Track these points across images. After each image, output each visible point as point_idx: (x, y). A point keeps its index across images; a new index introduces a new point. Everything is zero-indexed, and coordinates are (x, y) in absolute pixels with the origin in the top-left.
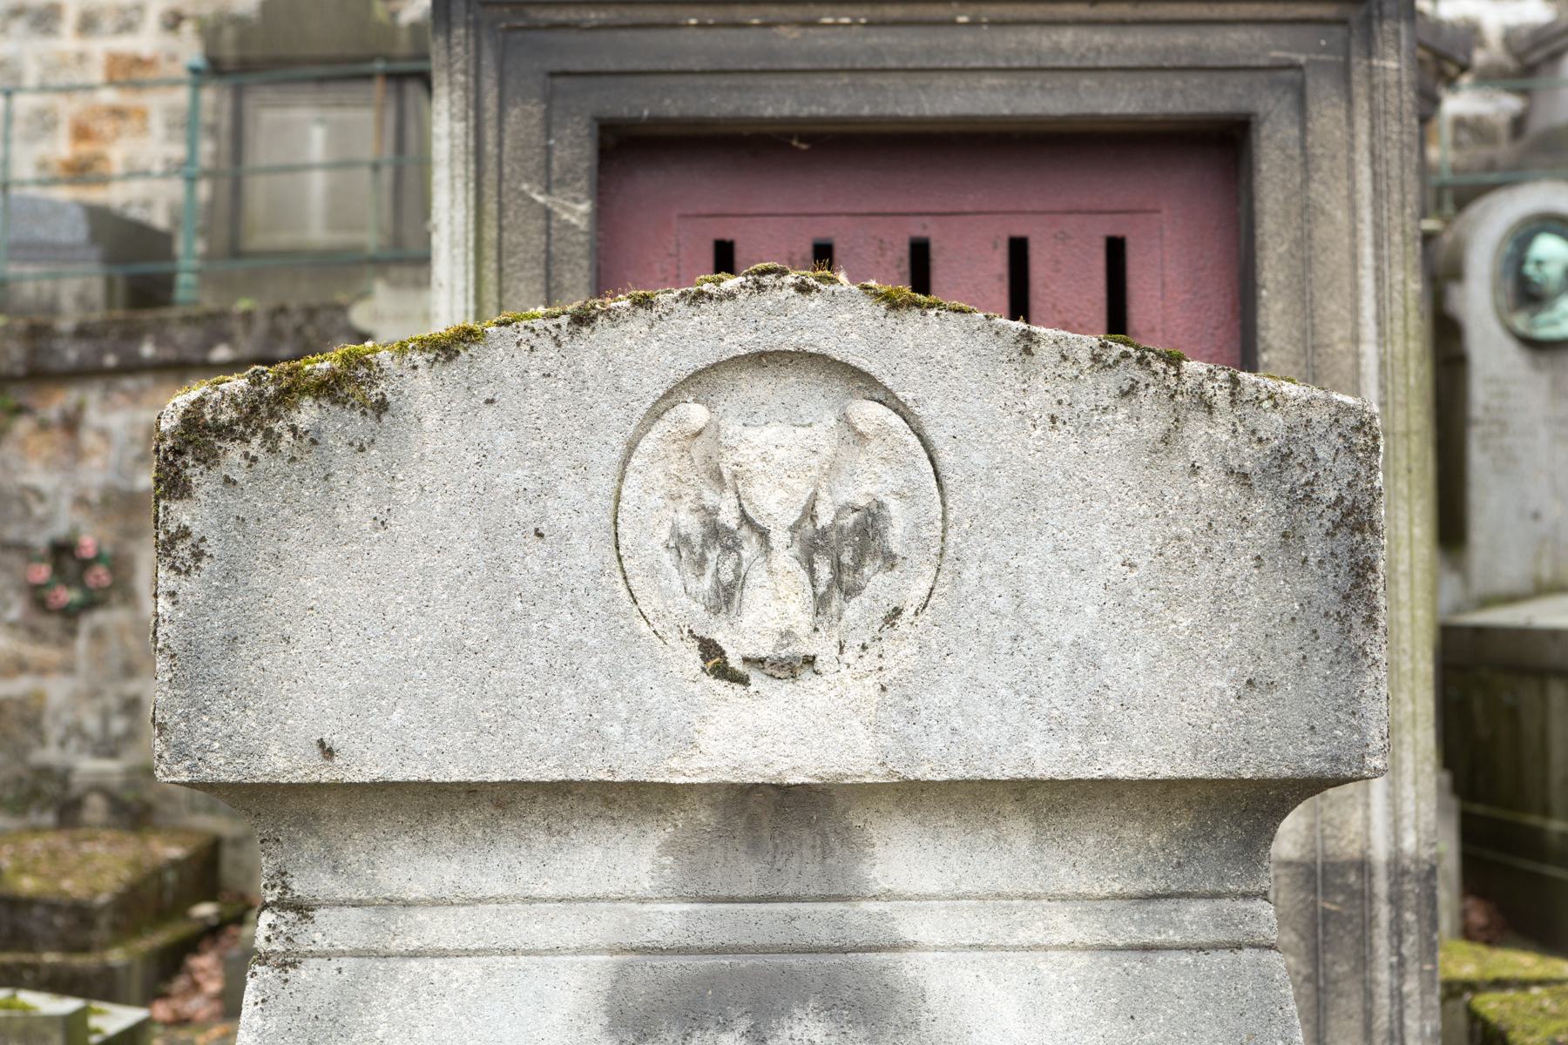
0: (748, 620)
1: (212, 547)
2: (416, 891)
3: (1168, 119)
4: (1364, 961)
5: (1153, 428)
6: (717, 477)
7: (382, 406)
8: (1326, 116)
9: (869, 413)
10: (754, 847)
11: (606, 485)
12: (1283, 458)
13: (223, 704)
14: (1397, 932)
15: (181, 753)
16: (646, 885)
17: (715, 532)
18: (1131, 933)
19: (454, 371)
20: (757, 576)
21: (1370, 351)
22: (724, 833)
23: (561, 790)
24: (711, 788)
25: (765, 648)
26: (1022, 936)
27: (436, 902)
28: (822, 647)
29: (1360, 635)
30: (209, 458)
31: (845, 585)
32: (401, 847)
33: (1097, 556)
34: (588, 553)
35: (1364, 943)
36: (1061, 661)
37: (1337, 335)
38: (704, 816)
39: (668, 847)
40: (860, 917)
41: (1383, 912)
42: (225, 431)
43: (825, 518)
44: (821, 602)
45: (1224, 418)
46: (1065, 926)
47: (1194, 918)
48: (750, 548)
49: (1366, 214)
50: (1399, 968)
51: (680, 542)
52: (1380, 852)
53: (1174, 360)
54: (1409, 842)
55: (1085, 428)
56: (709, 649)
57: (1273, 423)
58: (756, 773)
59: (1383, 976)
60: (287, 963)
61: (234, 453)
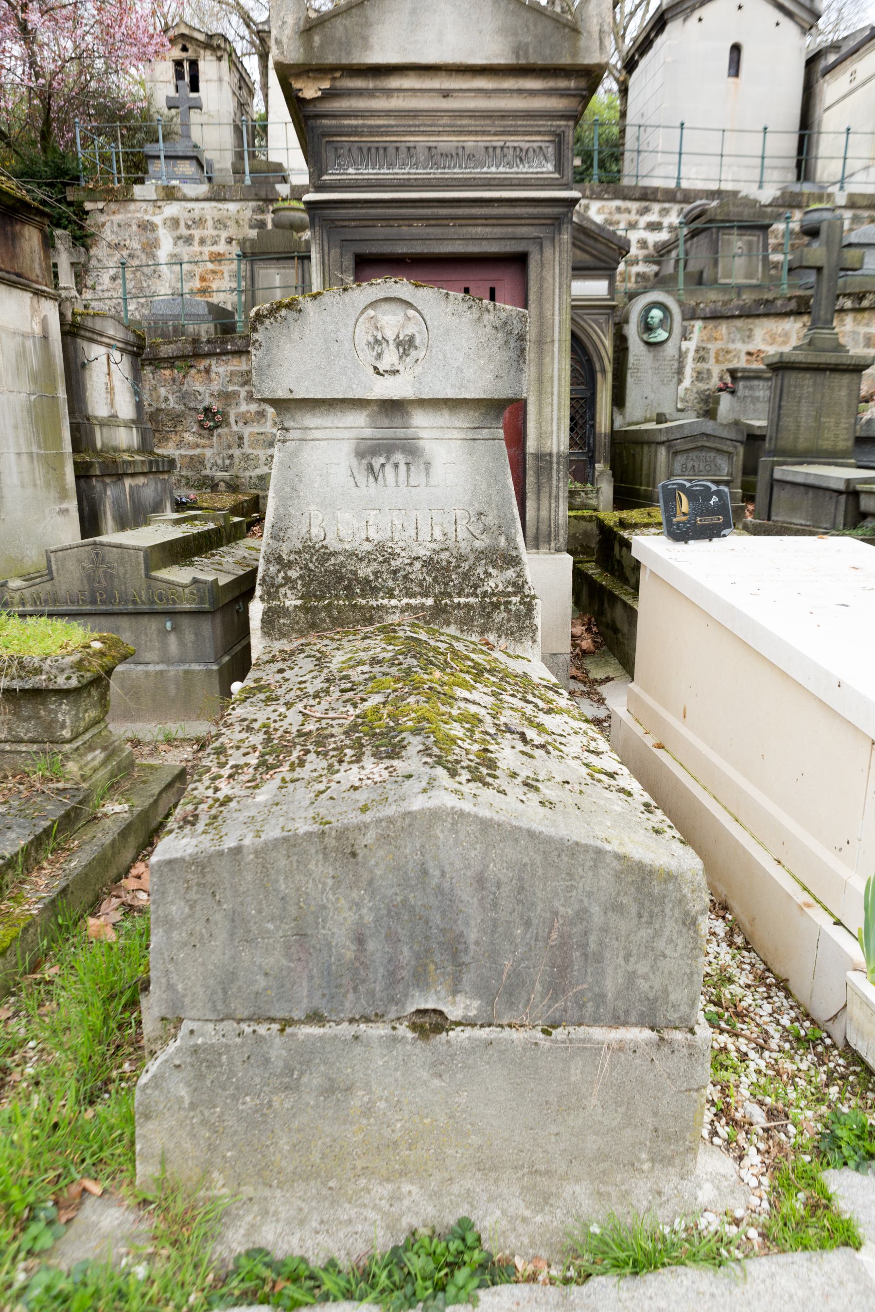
0: (384, 362)
1: (263, 344)
2: (312, 426)
3: (505, 253)
4: (550, 479)
5: (476, 316)
6: (377, 328)
7: (300, 311)
8: (548, 252)
9: (411, 313)
10: (387, 416)
11: (351, 329)
12: (505, 323)
13: (268, 380)
14: (558, 471)
15: (259, 391)
16: (363, 424)
17: (377, 341)
18: (470, 436)
19: (316, 302)
20: (386, 352)
21: (557, 318)
22: (380, 412)
23: (343, 401)
24: (376, 401)
25: (388, 368)
26: (446, 436)
27: (316, 428)
28: (401, 368)
29: (522, 365)
30: (262, 323)
31: (406, 354)
32: (308, 416)
33: (463, 347)
34: (348, 345)
35: (550, 474)
36: (454, 371)
37: (549, 314)
38: (376, 408)
39: (368, 416)
40: (410, 432)
41: (555, 466)
42: (265, 316)
43: (401, 338)
44: (401, 357)
45: (492, 314)
46: (456, 434)
47: (485, 433)
48: (384, 345)
49: (557, 280)
50: (558, 480)
51: (369, 343)
52: (555, 451)
53: (481, 300)
54: (562, 448)
55: (460, 316)
56: (375, 368)
57: (503, 315)
58: (386, 397)
59: (554, 482)
60: (284, 441)
61: (267, 321)
